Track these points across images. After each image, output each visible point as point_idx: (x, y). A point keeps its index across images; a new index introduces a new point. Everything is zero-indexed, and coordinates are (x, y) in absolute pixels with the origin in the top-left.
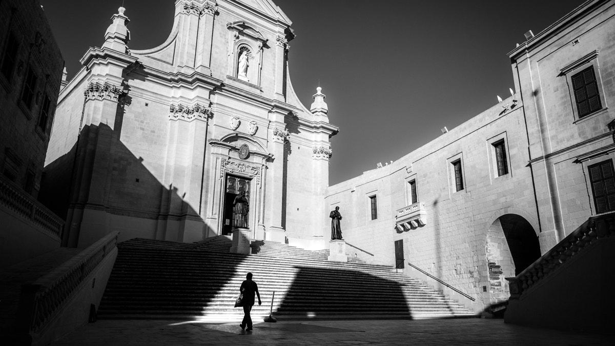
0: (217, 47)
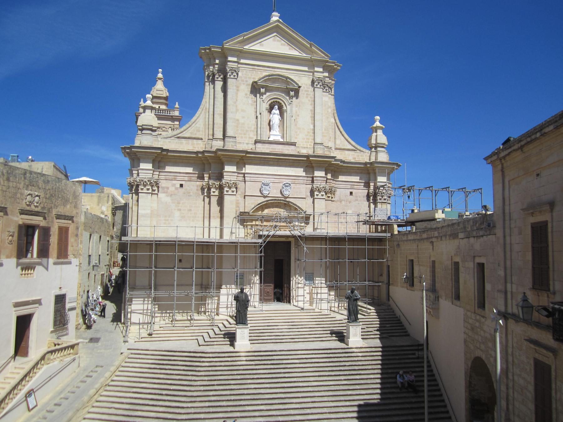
0: (243, 111)
